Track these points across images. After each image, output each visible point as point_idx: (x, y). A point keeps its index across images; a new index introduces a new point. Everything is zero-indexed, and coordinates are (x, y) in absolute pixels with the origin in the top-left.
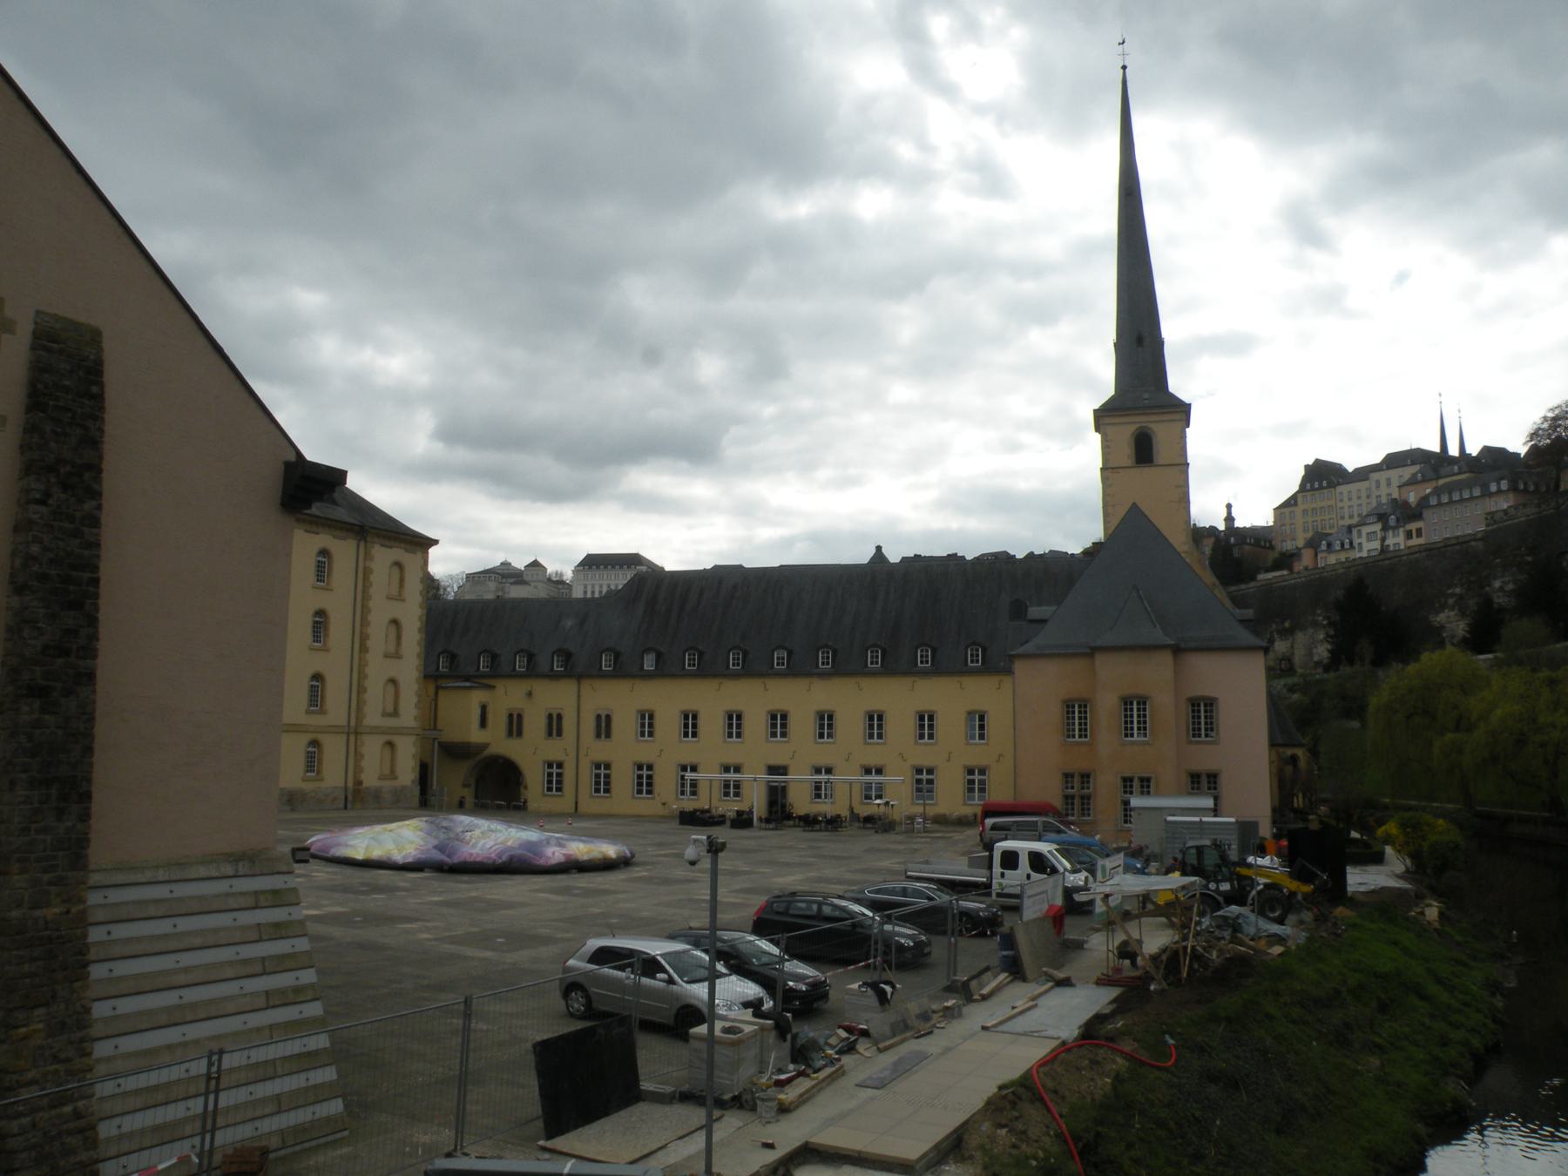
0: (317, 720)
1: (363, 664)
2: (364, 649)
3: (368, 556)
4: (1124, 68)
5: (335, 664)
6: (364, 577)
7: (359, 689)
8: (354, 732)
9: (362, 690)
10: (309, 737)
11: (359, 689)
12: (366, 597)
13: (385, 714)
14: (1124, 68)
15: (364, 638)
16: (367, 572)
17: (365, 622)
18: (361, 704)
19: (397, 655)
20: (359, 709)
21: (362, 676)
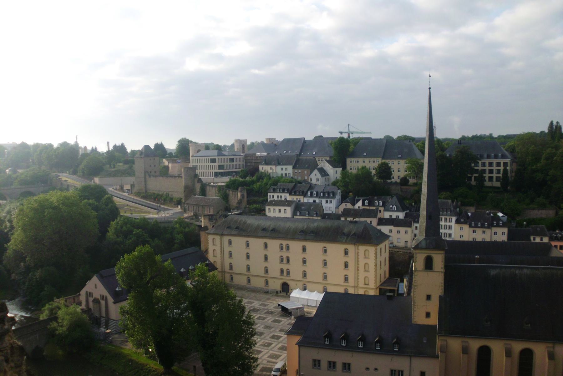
0: (346, 284)
1: (358, 273)
2: (358, 270)
3: (358, 249)
4: (430, 88)
5: (351, 273)
6: (357, 255)
7: (357, 278)
8: (355, 287)
9: (358, 279)
10: (345, 287)
11: (357, 278)
12: (358, 258)
13: (365, 284)
14: (430, 88)
15: (358, 267)
16: (358, 253)
17: (358, 264)
18: (358, 282)
19: (368, 271)
20: (358, 284)
21: (358, 276)
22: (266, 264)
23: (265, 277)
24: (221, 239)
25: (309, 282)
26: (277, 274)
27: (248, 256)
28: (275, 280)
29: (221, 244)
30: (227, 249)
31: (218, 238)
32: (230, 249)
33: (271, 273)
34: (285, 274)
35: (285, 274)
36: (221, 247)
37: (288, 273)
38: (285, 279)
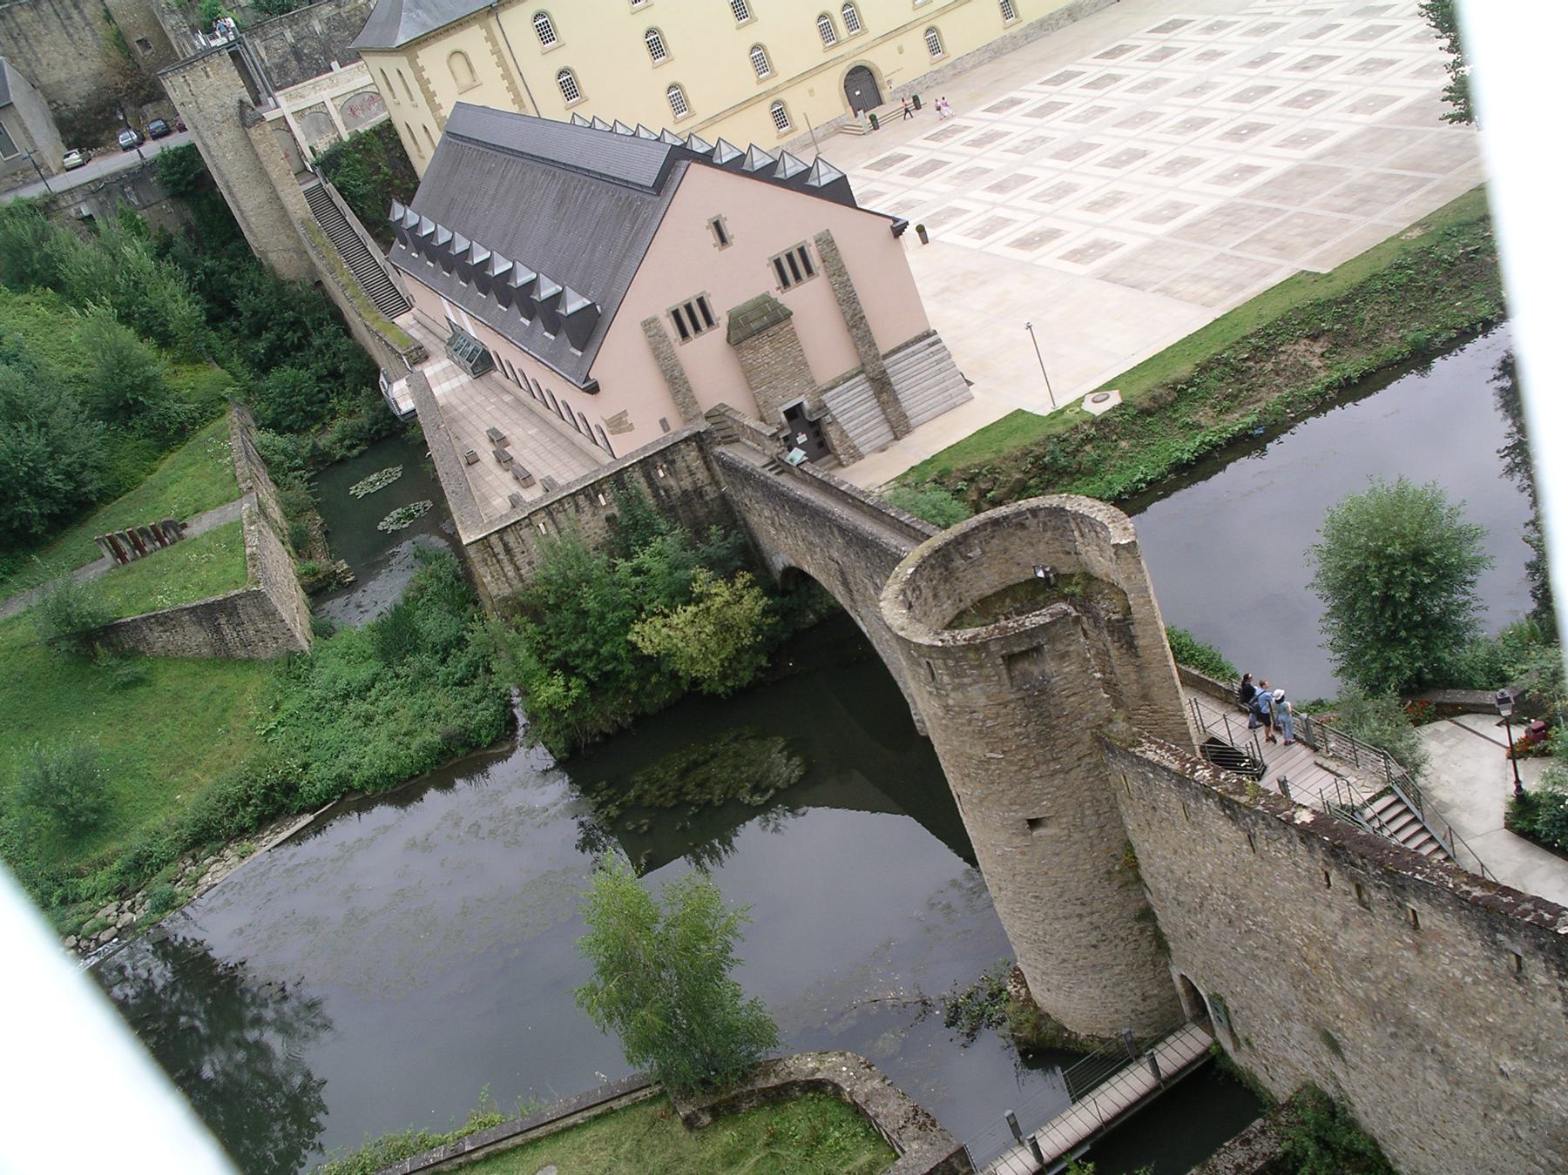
22: (752, 34)
23: (767, 94)
24: (491, 38)
25: (944, 10)
26: (812, 49)
27: (656, 45)
28: (816, 82)
29: (501, 63)
30: (539, 68)
31: (472, 39)
32: (560, 60)
33: (786, 64)
34: (842, 29)
35: (842, 29)
36: (507, 75)
37: (853, 21)
38: (852, 51)
